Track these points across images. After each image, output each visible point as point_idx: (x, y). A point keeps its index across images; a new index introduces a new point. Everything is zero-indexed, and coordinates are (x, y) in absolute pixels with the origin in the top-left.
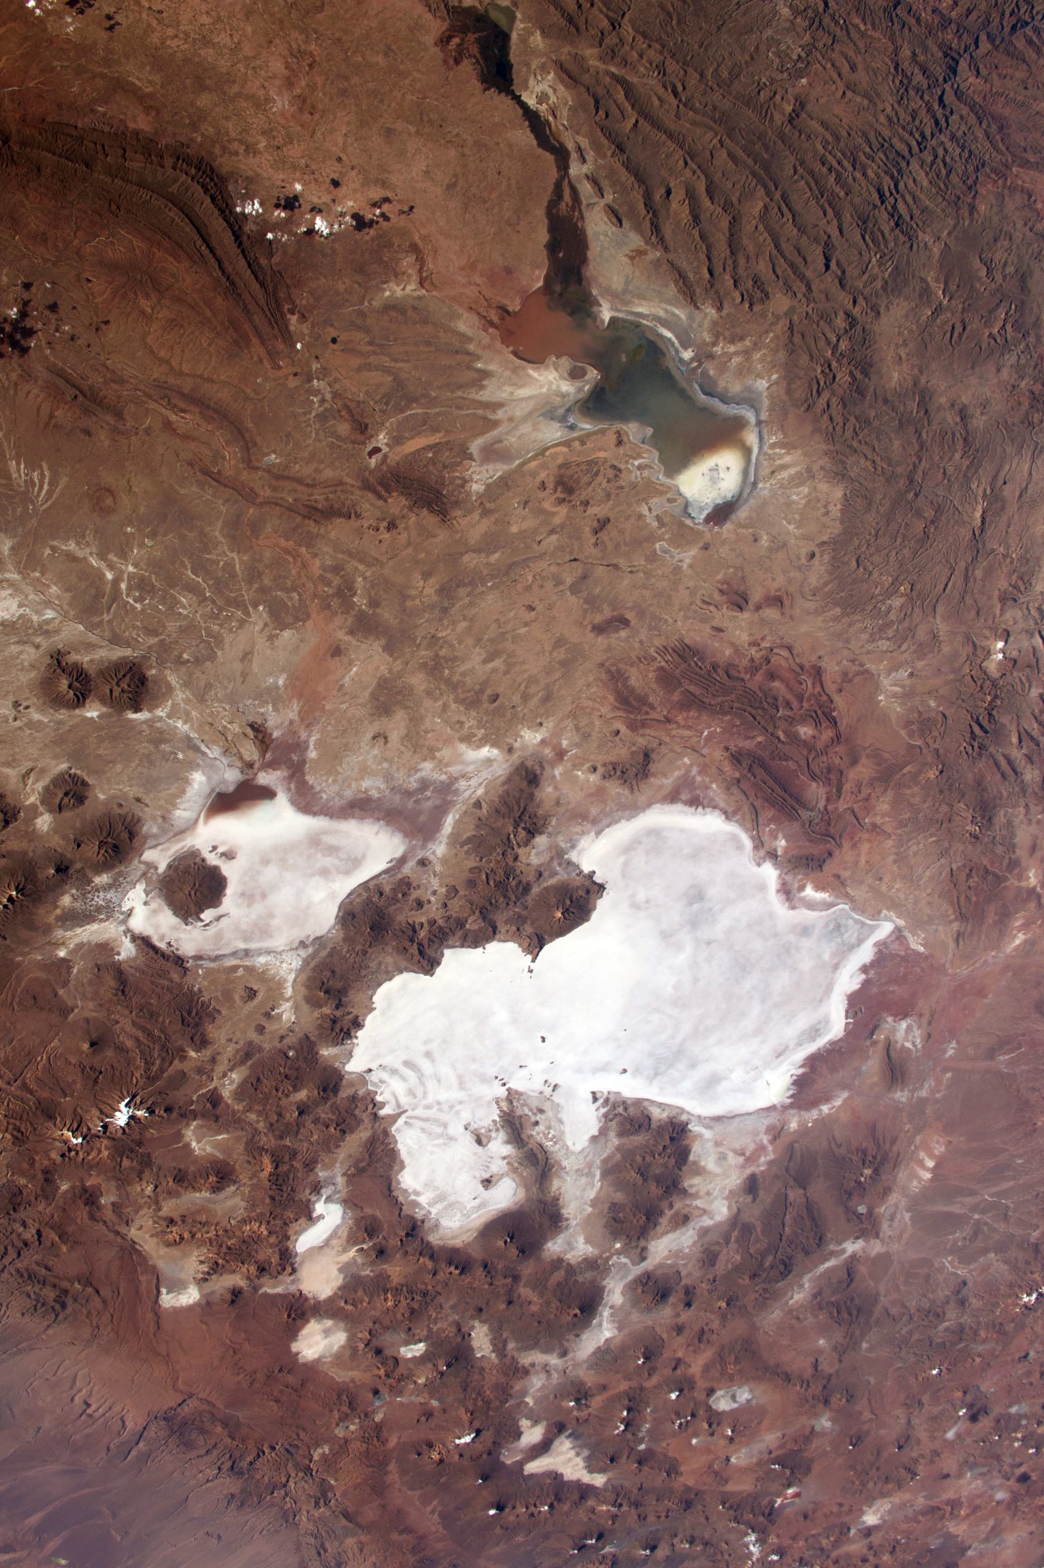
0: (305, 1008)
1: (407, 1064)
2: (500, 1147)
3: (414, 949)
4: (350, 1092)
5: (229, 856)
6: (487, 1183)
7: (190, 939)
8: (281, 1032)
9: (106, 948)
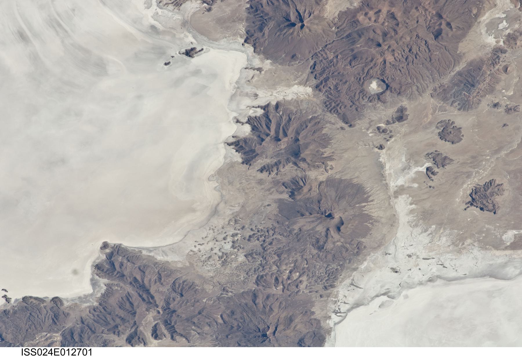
0: (364, 177)
3: (160, 292)
8: (401, 128)
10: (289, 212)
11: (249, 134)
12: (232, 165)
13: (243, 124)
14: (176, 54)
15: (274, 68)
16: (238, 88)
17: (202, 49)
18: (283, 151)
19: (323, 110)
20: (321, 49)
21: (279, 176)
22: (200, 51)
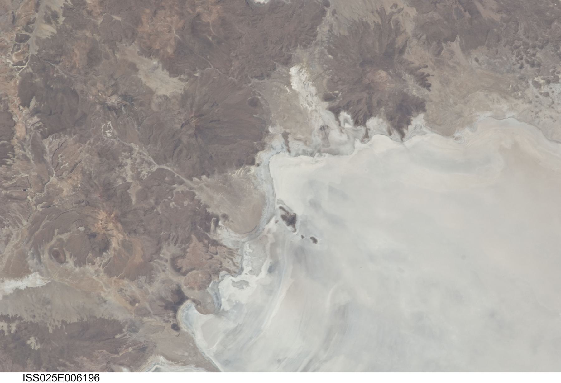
4: (217, 203)
10: (478, 35)
11: (379, 117)
12: (432, 123)
13: (367, 130)
14: (297, 235)
15: (277, 121)
16: (319, 151)
17: (281, 208)
18: (391, 71)
19: (316, 44)
20: (231, 78)
21: (427, 64)
22: (284, 210)
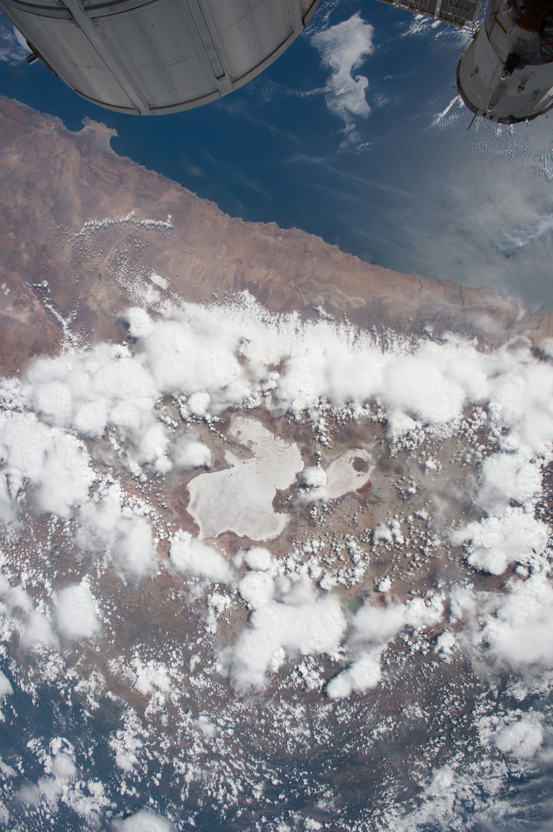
1: (283, 451)
2: (244, 442)
5: (359, 476)
6: (240, 433)
7: (352, 454)
9: (368, 443)
